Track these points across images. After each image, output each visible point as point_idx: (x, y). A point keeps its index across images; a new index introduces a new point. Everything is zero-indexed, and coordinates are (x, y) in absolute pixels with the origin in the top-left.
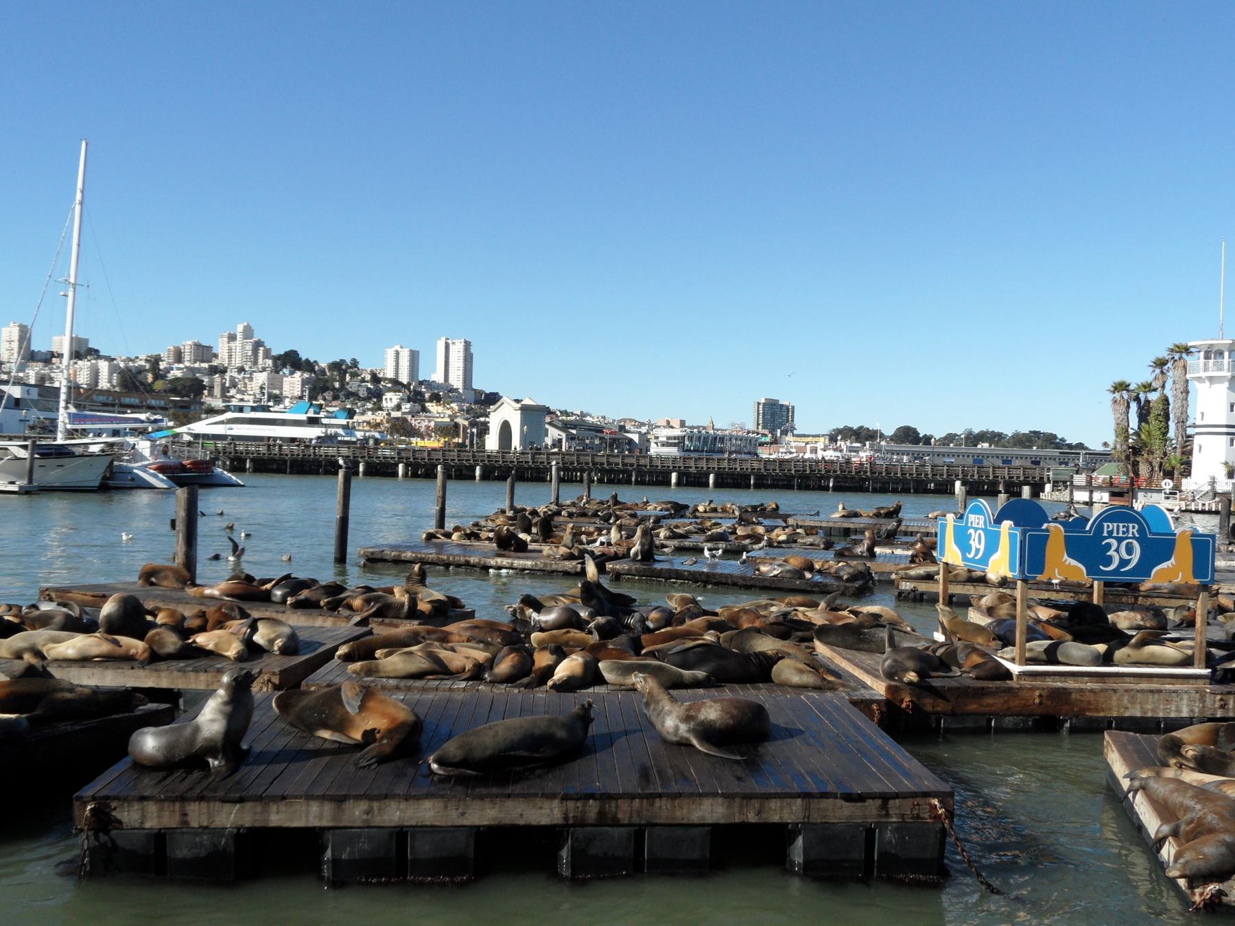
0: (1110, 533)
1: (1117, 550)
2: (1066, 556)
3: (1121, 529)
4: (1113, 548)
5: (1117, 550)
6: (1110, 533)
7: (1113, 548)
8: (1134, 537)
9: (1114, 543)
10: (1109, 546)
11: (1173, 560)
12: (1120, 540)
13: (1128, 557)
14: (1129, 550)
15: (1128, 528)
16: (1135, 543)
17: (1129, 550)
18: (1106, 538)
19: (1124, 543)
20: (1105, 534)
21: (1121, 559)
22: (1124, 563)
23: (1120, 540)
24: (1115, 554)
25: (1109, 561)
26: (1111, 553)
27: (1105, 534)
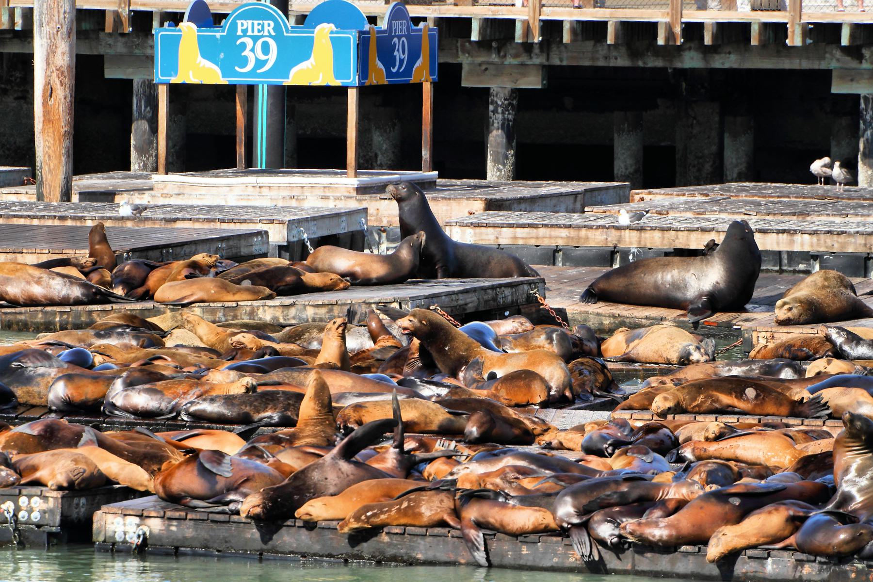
0: (245, 31)
1: (253, 50)
2: (199, 58)
3: (256, 27)
6: (245, 31)
8: (270, 36)
9: (249, 42)
10: (243, 46)
11: (312, 59)
12: (255, 39)
13: (262, 57)
14: (266, 48)
16: (271, 42)
17: (266, 48)
18: (240, 37)
19: (259, 43)
21: (256, 58)
22: (260, 63)
23: (255, 39)
25: (244, 61)
26: (246, 53)
27: (239, 33)
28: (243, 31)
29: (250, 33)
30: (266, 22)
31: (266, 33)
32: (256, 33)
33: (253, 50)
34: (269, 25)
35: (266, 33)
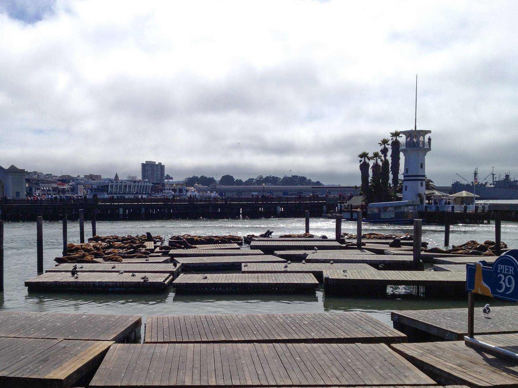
0: (501, 270)
3: (506, 269)
4: (503, 280)
5: (504, 281)
6: (501, 270)
7: (503, 280)
8: (512, 275)
12: (506, 275)
13: (509, 286)
14: (510, 282)
15: (509, 268)
17: (510, 282)
19: (507, 278)
20: (499, 271)
21: (506, 286)
22: (507, 289)
23: (506, 275)
24: (503, 283)
25: (500, 287)
27: (499, 271)
28: (500, 270)
29: (503, 272)
30: (510, 267)
31: (510, 273)
32: (506, 272)
33: (504, 281)
34: (512, 269)
35: (510, 273)
